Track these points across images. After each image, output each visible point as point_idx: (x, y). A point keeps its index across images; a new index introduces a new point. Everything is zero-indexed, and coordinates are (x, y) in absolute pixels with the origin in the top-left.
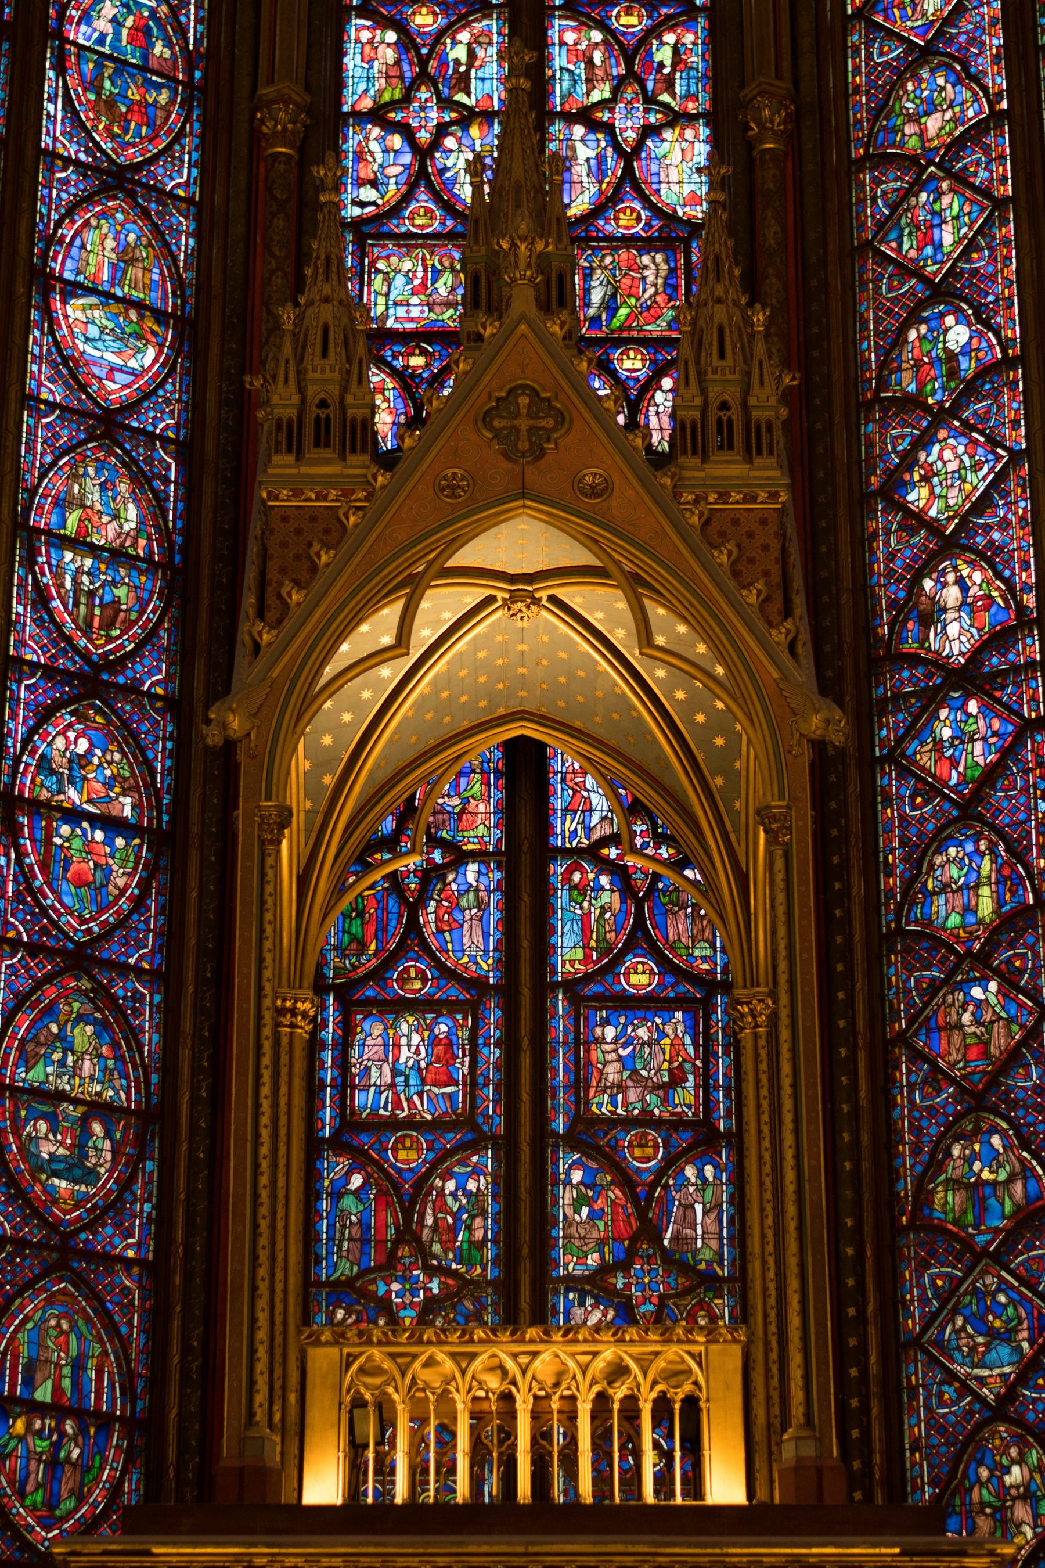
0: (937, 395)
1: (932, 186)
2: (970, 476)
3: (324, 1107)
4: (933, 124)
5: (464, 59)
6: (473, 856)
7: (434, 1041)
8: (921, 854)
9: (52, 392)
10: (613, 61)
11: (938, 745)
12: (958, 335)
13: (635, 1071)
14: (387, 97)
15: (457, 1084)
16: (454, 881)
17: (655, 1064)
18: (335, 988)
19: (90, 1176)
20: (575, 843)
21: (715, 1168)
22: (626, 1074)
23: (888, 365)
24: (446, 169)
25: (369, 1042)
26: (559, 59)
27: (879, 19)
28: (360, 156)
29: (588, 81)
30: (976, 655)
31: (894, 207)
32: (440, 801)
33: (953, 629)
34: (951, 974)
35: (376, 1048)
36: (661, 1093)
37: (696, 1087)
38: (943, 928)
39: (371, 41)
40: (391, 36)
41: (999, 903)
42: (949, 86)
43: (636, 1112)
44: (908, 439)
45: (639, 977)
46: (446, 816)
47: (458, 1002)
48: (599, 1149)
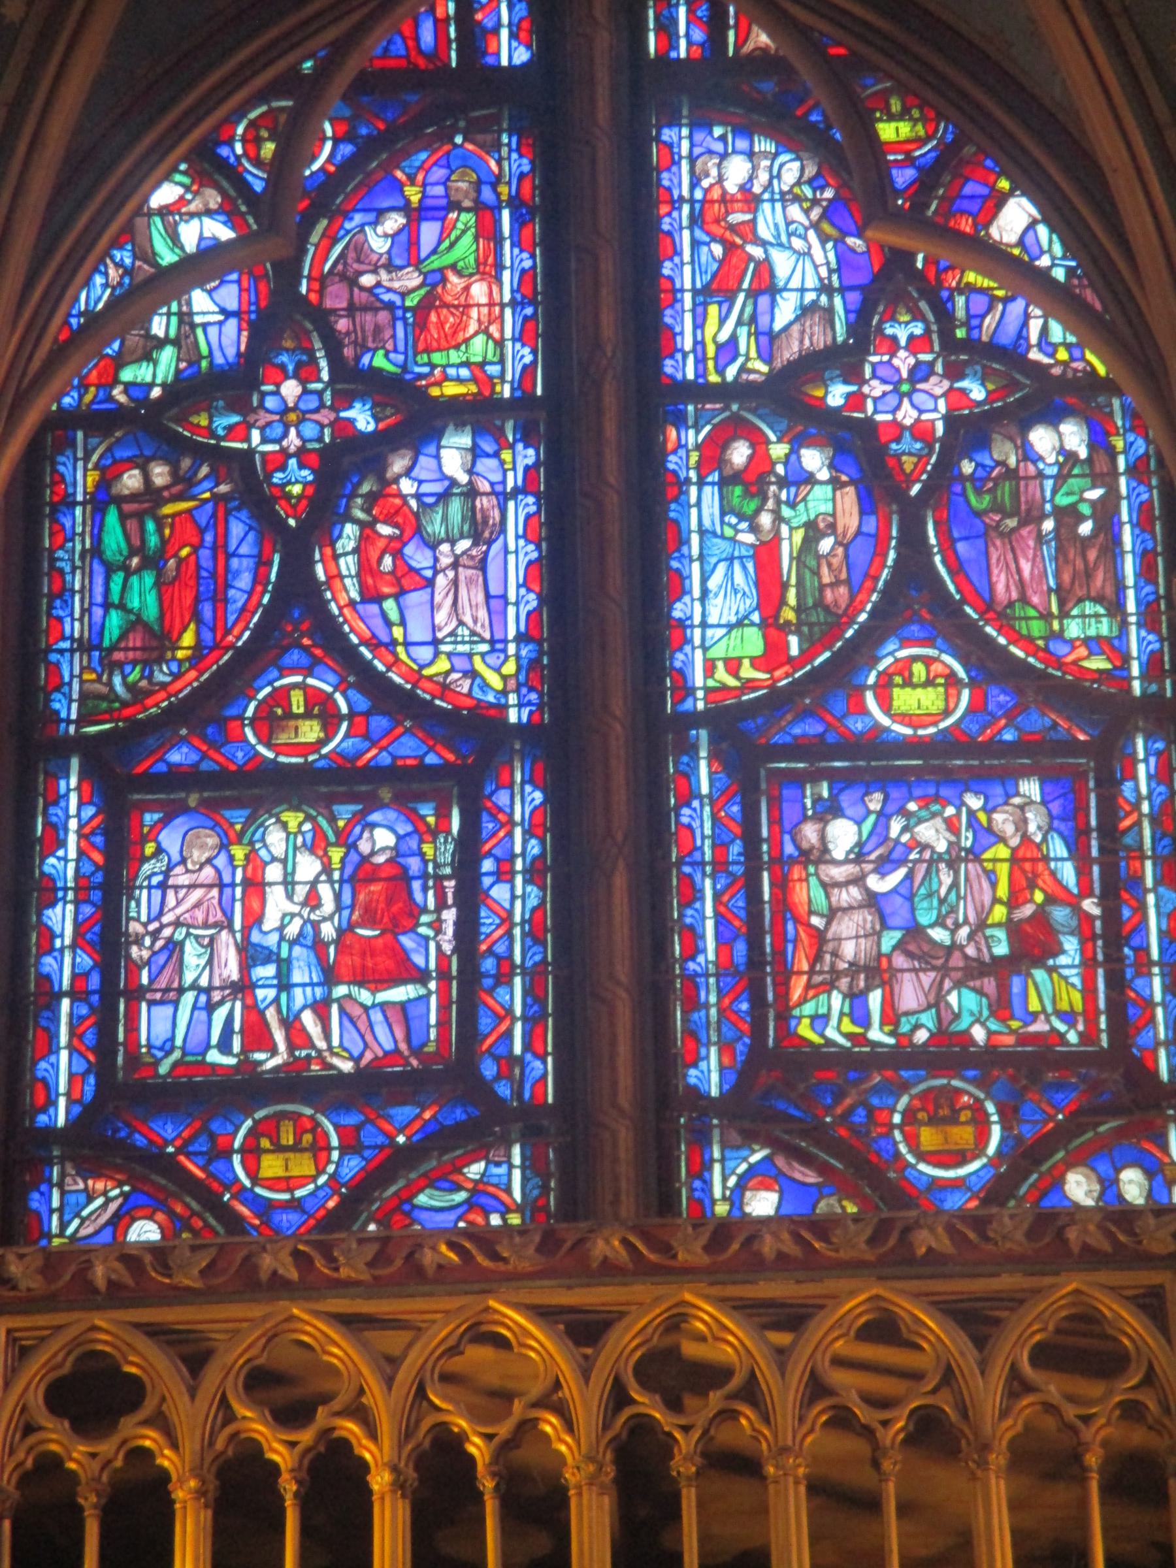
3: (51, 1048)
7: (361, 873)
13: (914, 931)
15: (421, 976)
16: (408, 472)
17: (966, 911)
18: (82, 745)
20: (731, 373)
21: (1150, 1174)
22: (890, 940)
25: (181, 878)
32: (367, 280)
35: (197, 894)
36: (990, 984)
37: (1088, 965)
43: (922, 1036)
45: (917, 696)
46: (383, 316)
47: (422, 770)
48: (816, 1133)
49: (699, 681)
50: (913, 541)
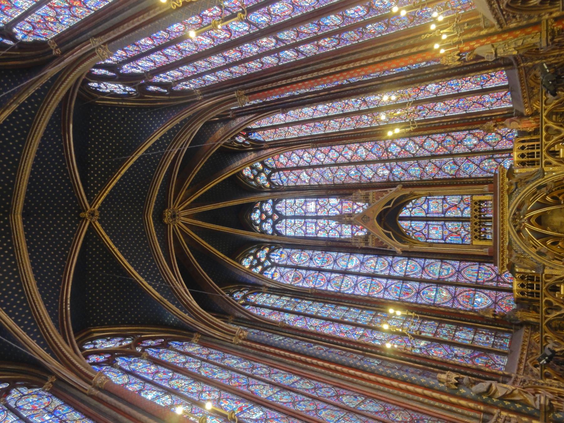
0: (359, 174)
4: (330, 175)
9: (358, 269)
12: (353, 172)
19: (449, 268)
26: (322, 214)
45: (425, 206)
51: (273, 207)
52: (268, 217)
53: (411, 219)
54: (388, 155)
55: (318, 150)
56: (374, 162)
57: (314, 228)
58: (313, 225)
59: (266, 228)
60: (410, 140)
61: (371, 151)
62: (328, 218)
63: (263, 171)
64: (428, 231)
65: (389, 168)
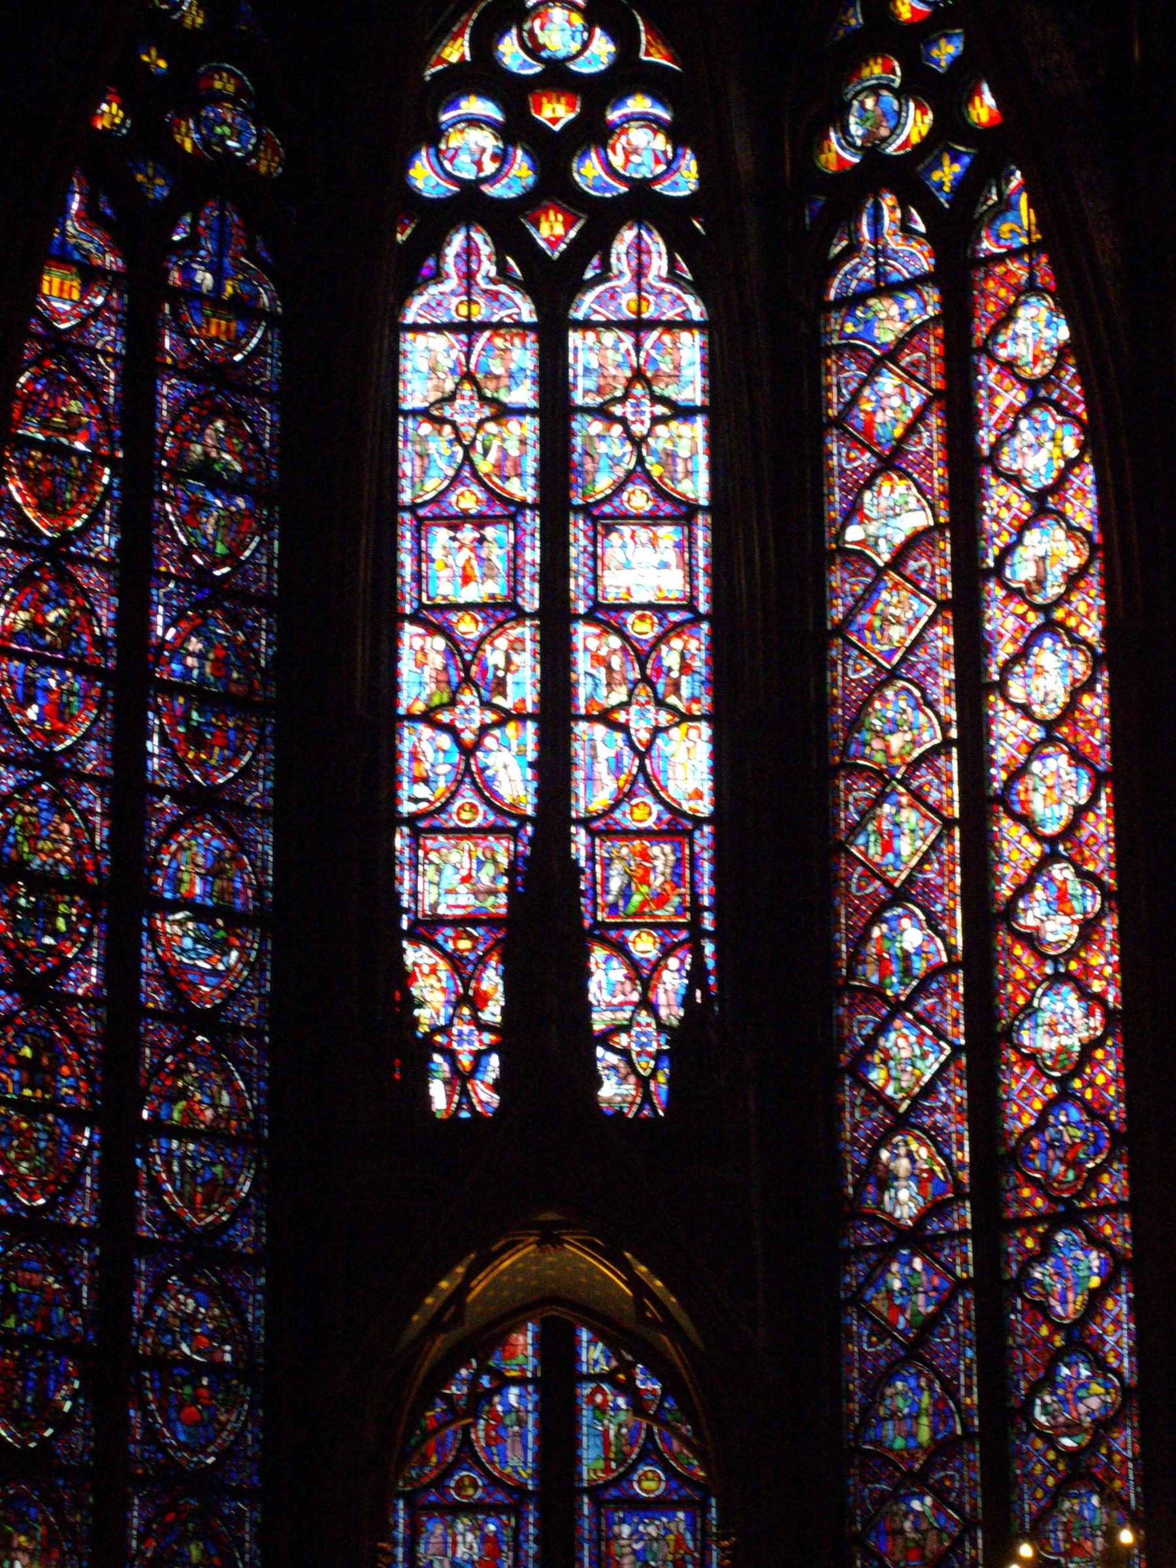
0: (895, 988)
1: (894, 798)
2: (919, 1063)
4: (896, 742)
5: (502, 664)
6: (514, 1381)
7: (484, 1539)
8: (876, 1386)
10: (629, 665)
11: (890, 1292)
12: (912, 937)
14: (436, 701)
17: (660, 1556)
23: (856, 957)
24: (487, 768)
25: (432, 1540)
26: (583, 663)
27: (854, 639)
28: (414, 757)
29: (609, 685)
30: (921, 1219)
31: (862, 814)
33: (904, 1195)
34: (896, 1488)
38: (891, 1450)
39: (422, 649)
40: (440, 643)
41: (934, 1430)
42: (909, 710)
44: (871, 1025)
45: (649, 1483)
49: (585, 1476)
50: (649, 1430)
51: (641, 203)
52: (553, 154)
53: (557, 1383)
54: (1028, 1224)
55: (1097, 663)
56: (985, 1109)
57: (473, 593)
58: (496, 588)
59: (455, 140)
60: (1126, 1391)
61: (1066, 1096)
62: (555, 714)
63: (950, 129)
64: (472, 1509)
65: (935, 1226)
